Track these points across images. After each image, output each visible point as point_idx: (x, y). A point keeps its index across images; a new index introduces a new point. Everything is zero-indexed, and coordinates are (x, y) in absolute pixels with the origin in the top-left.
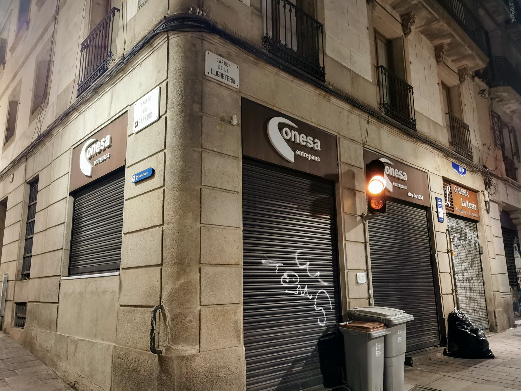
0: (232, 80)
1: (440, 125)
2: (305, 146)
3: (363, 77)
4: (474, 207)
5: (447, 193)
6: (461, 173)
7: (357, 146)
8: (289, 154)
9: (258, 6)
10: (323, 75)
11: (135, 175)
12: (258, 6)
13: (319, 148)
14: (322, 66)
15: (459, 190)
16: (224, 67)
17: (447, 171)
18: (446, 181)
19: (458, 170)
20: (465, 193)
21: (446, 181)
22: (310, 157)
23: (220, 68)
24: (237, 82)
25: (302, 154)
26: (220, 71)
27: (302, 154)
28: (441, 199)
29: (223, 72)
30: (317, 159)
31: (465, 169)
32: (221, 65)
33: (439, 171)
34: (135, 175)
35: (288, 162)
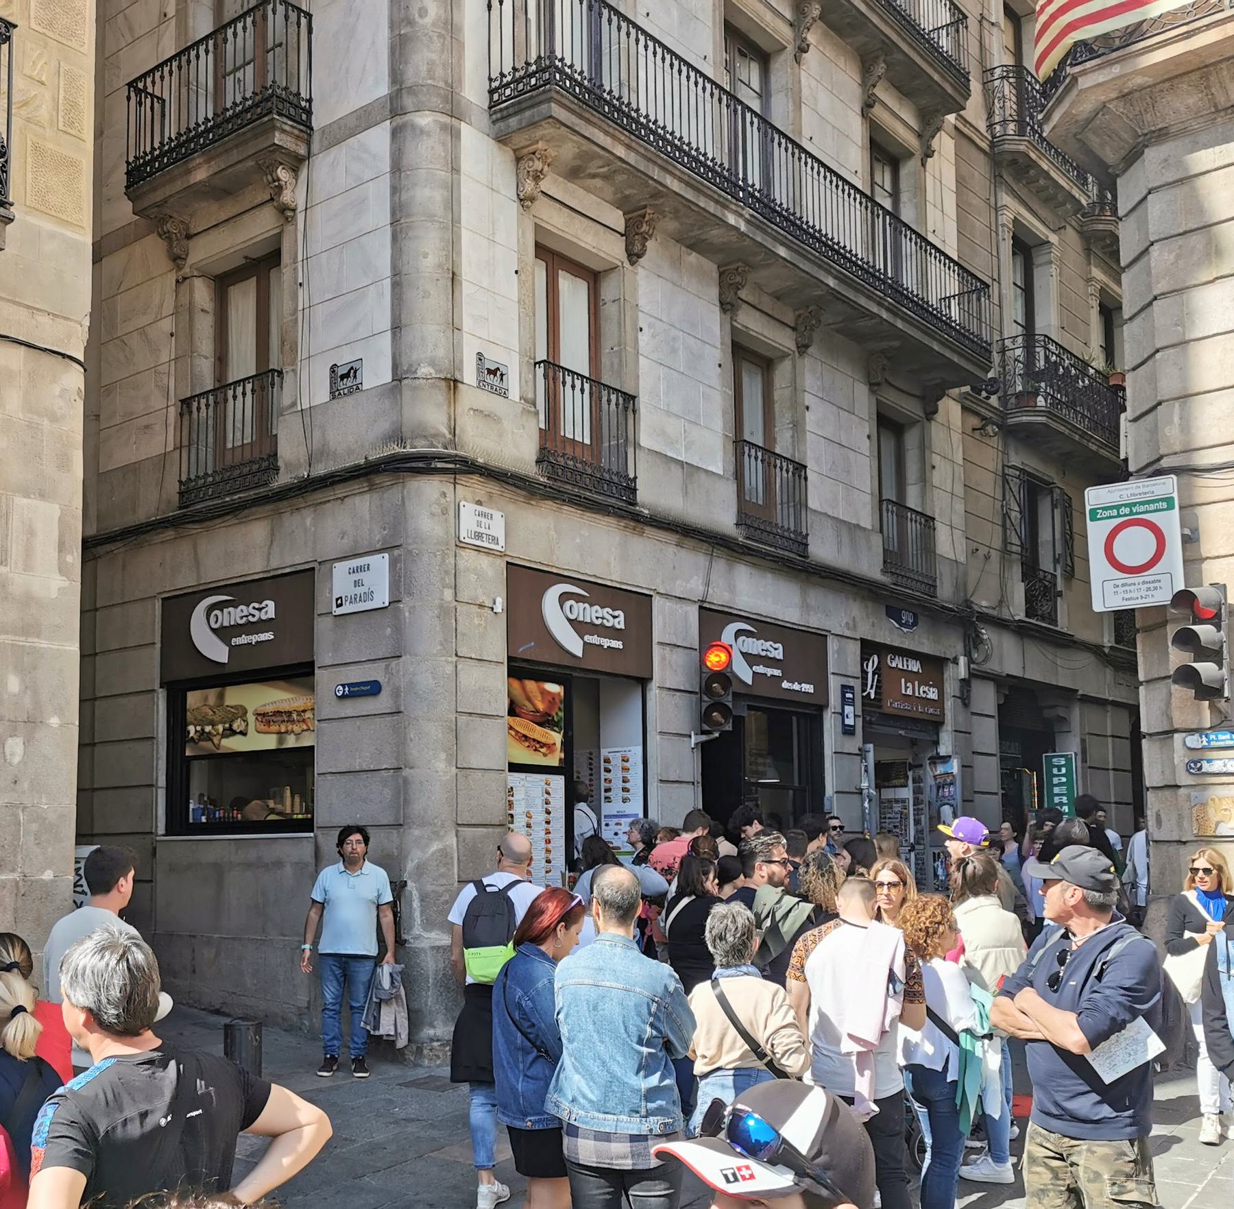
0: (495, 540)
1: (865, 529)
2: (601, 624)
3: (706, 471)
4: (933, 694)
5: (870, 670)
6: (906, 625)
7: (689, 608)
8: (574, 644)
9: (530, 396)
10: (634, 490)
11: (343, 686)
12: (530, 396)
13: (622, 626)
14: (632, 476)
15: (897, 663)
16: (484, 520)
17: (873, 625)
18: (868, 648)
19: (899, 621)
20: (915, 666)
21: (868, 648)
22: (606, 643)
23: (479, 524)
24: (502, 542)
25: (594, 639)
26: (479, 530)
27: (594, 639)
28: (852, 688)
29: (482, 530)
30: (617, 644)
31: (915, 616)
32: (480, 519)
33: (855, 628)
34: (343, 686)
35: (575, 656)
